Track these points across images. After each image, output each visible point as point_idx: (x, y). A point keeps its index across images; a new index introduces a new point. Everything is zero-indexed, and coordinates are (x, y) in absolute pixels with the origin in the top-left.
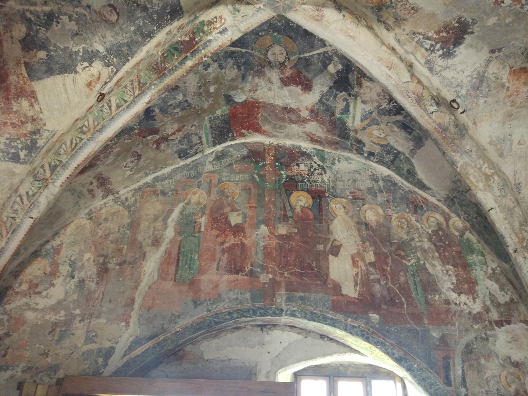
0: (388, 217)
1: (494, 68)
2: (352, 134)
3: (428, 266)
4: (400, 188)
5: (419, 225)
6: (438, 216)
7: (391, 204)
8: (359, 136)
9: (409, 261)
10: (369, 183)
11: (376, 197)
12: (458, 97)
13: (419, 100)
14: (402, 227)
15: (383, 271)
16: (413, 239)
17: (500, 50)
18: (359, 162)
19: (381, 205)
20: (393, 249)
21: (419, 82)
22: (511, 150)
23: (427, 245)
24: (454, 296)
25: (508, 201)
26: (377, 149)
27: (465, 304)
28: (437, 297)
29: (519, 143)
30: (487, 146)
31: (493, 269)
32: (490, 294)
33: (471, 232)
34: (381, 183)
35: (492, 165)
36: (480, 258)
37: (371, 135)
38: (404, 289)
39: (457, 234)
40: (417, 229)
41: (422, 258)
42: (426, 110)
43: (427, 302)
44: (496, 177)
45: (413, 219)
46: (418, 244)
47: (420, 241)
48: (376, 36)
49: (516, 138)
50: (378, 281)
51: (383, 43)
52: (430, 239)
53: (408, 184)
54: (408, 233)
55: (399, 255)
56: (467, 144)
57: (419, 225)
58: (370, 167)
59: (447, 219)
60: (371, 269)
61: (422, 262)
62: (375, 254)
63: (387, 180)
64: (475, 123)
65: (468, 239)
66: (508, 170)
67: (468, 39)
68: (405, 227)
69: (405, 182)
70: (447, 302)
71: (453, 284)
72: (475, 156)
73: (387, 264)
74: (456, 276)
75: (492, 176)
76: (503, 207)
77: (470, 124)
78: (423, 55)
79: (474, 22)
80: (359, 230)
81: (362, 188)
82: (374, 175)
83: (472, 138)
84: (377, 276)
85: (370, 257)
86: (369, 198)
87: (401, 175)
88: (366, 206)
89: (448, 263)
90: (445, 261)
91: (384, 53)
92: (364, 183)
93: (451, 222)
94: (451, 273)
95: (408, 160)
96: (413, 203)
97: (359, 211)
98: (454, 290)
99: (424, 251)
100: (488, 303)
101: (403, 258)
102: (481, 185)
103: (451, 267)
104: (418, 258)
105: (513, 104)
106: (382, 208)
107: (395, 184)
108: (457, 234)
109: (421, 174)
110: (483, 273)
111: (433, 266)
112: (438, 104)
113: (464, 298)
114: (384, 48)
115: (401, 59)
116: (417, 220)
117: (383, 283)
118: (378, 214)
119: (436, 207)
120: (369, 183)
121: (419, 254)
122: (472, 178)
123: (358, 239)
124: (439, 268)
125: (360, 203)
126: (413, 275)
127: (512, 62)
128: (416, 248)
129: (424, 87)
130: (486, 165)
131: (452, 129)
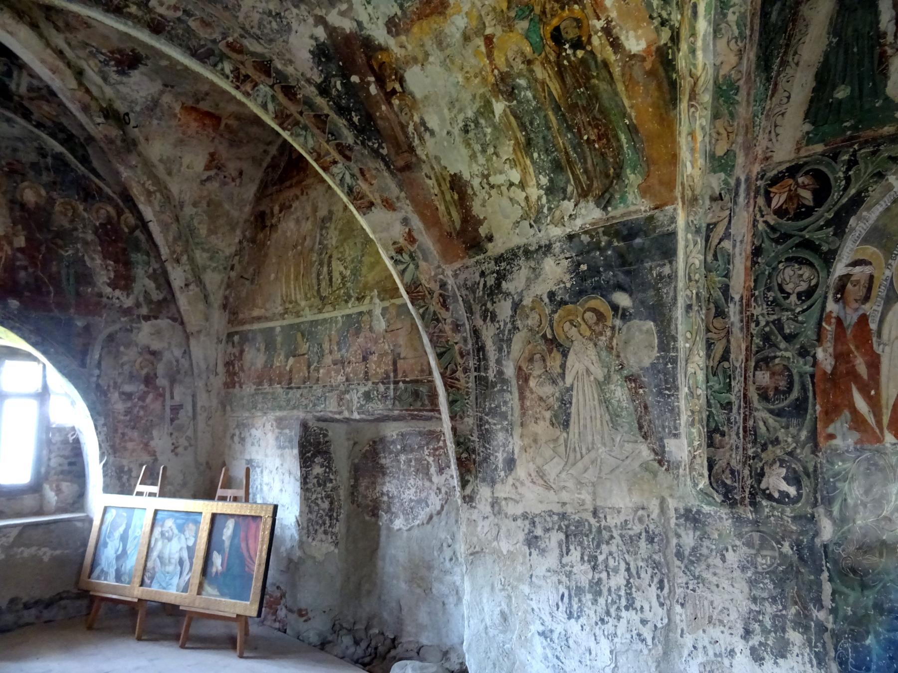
0: (51, 201)
1: (166, 99)
2: (16, 98)
3: (86, 258)
4: (72, 170)
5: (86, 215)
6: (110, 209)
7: (59, 187)
8: (26, 103)
9: (67, 251)
10: (33, 157)
11: (41, 175)
12: (132, 111)
13: (85, 109)
14: (66, 215)
15: (32, 259)
16: (76, 229)
17: (172, 87)
18: (24, 127)
19: (45, 186)
20: (50, 237)
21: (88, 91)
22: (179, 171)
23: (90, 237)
24: (108, 290)
25: (167, 217)
26: (49, 124)
27: (118, 298)
28: (89, 290)
29: (188, 167)
30: (156, 162)
31: (154, 270)
32: (146, 292)
33: (141, 231)
34: (49, 160)
35: (156, 180)
36: (145, 257)
37: (40, 107)
38: (55, 280)
39: (126, 230)
40: (84, 219)
41: (82, 250)
42: (92, 121)
43: (78, 294)
44: (158, 195)
45: (81, 207)
46: (81, 235)
47: (84, 232)
48: (41, 36)
49: (186, 161)
50: (25, 268)
51: (48, 44)
52: (96, 232)
53: (83, 168)
54: (72, 221)
55: (56, 244)
56: (133, 160)
57: (86, 215)
58: (38, 138)
59: (120, 213)
60: (19, 255)
61: (80, 254)
62: (27, 240)
63: (58, 157)
64: (147, 140)
65: (137, 237)
66: (175, 188)
67: (142, 68)
68: (70, 214)
69: (80, 165)
70: (100, 295)
71: (109, 278)
72: (139, 172)
73: (39, 251)
74: (115, 272)
75: (154, 192)
76: (162, 223)
77: (142, 139)
78: (96, 65)
79: (147, 57)
80: (11, 210)
81: (24, 160)
82: (42, 148)
83: (140, 154)
84: (25, 263)
85: (20, 241)
86: (31, 173)
87: (76, 157)
88: (26, 184)
89: (110, 259)
90: (105, 256)
91: (49, 55)
92: (29, 156)
93: (122, 218)
94: (110, 268)
95: (83, 146)
96: (84, 189)
97: (15, 188)
98: (109, 285)
99: (86, 243)
100: (141, 299)
101: (61, 247)
102: (142, 199)
103: (112, 263)
104: (78, 250)
105: (184, 133)
106: (45, 189)
107: (66, 164)
108: (126, 230)
109: (96, 164)
110: (143, 272)
111: (93, 259)
112: (106, 117)
113: (118, 293)
114: (49, 51)
115: (69, 65)
116: (85, 210)
117: (31, 270)
118: (40, 195)
119: (110, 200)
120: (33, 157)
121: (79, 246)
122: (135, 190)
123: (9, 221)
124: (99, 262)
125: (18, 178)
126: (68, 267)
127: (183, 99)
128: (77, 238)
129: (93, 98)
130: (150, 182)
131: (119, 143)
